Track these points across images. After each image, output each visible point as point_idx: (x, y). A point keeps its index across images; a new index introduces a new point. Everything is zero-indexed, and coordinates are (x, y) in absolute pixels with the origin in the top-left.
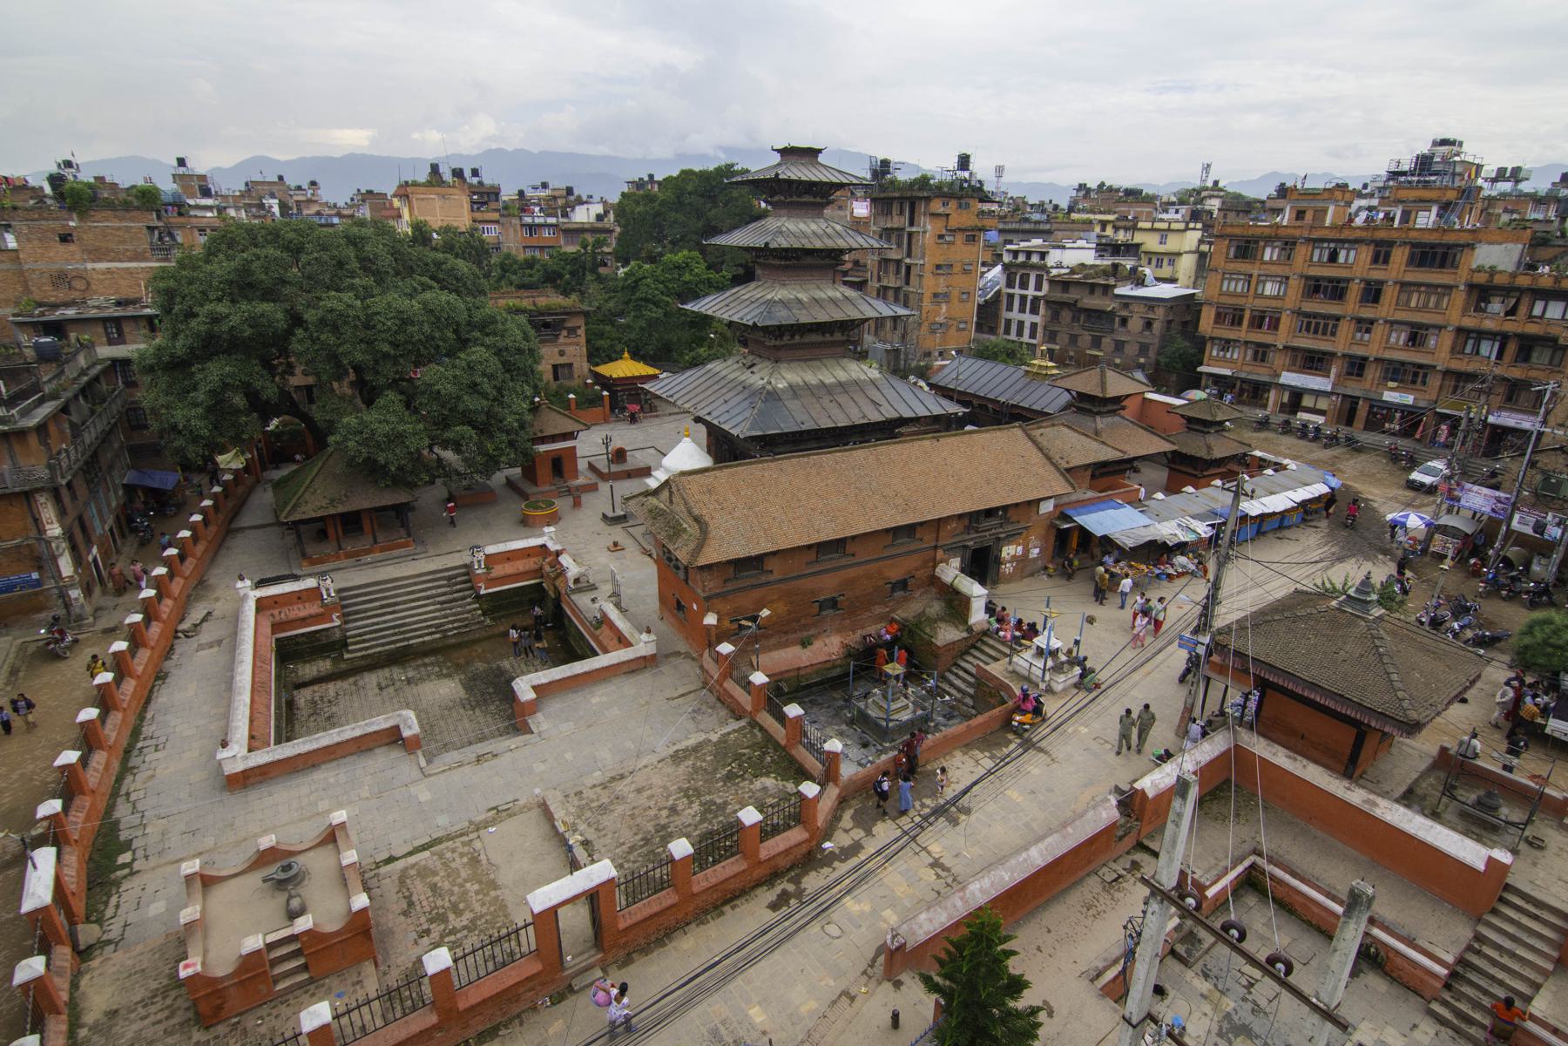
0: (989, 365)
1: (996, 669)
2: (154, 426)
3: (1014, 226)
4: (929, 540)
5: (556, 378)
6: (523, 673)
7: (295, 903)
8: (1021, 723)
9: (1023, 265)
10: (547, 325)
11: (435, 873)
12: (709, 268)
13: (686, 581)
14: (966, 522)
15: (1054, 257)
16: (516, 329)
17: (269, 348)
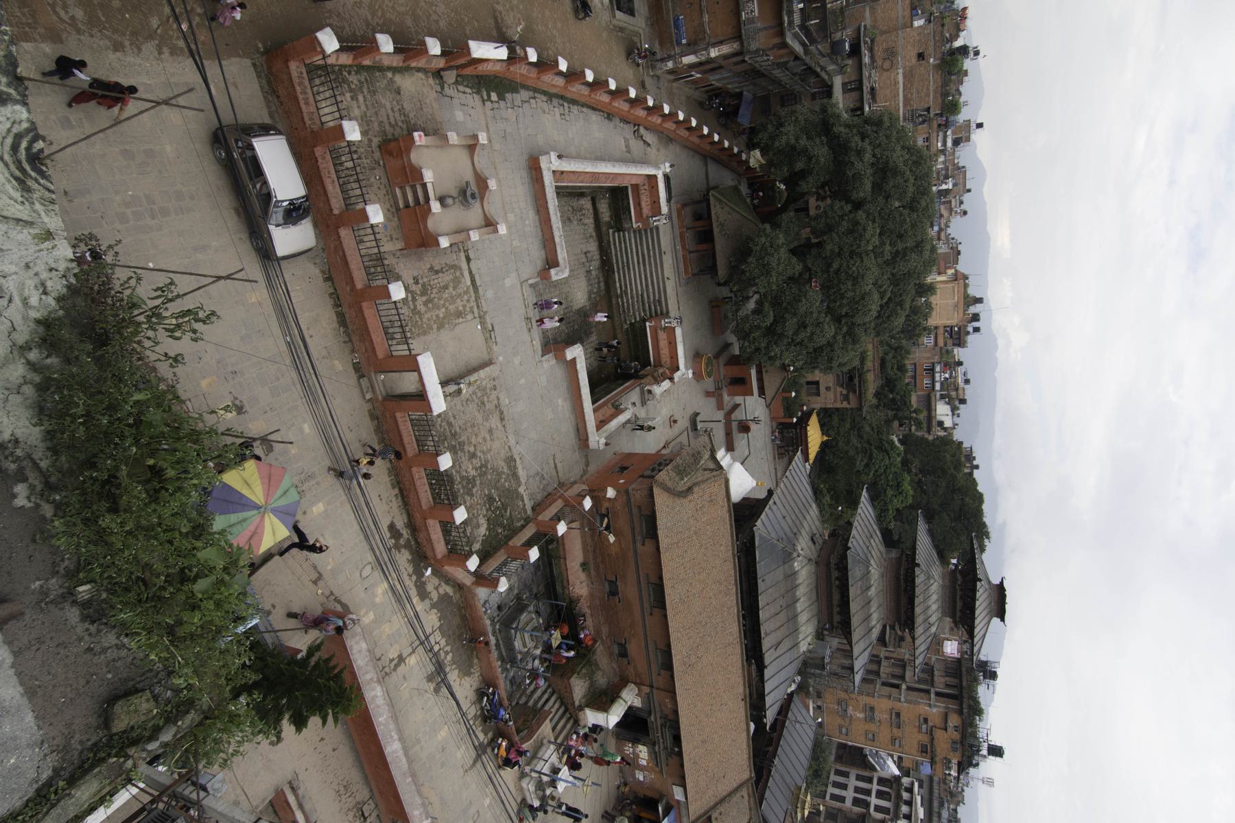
0: (808, 753)
1: (546, 728)
2: (783, 112)
3: (936, 792)
4: (659, 681)
5: (808, 383)
6: (585, 350)
7: (450, 201)
8: (499, 746)
9: (899, 796)
10: (852, 380)
11: (455, 288)
12: (898, 510)
13: (642, 476)
14: (671, 717)
16: (849, 358)
17: (838, 184)
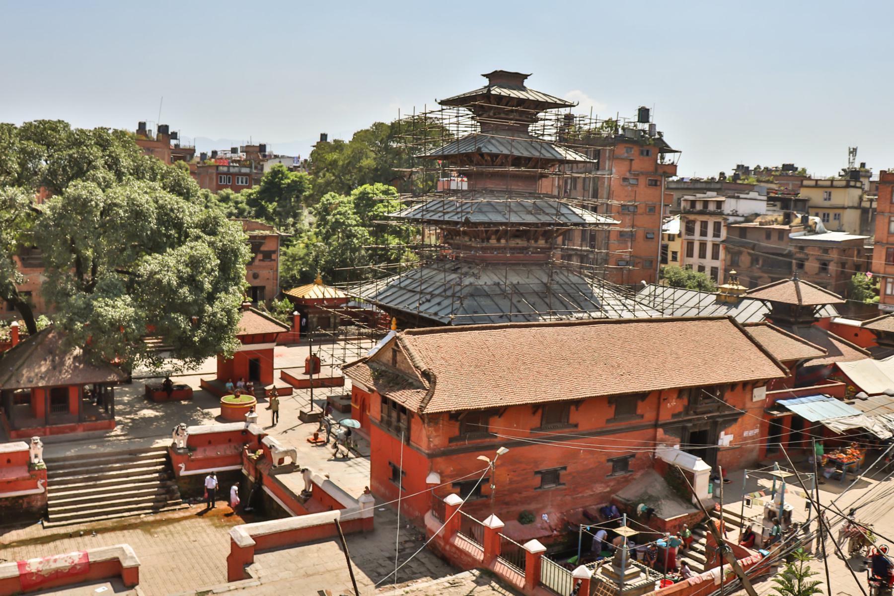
15: (729, 206)
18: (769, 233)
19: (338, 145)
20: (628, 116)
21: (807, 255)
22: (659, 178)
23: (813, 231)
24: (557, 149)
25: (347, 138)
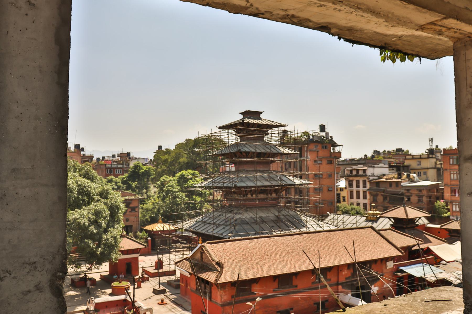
15: (370, 171)
18: (391, 184)
19: (168, 152)
20: (314, 130)
21: (411, 193)
22: (332, 160)
23: (413, 181)
24: (278, 148)
25: (172, 148)
